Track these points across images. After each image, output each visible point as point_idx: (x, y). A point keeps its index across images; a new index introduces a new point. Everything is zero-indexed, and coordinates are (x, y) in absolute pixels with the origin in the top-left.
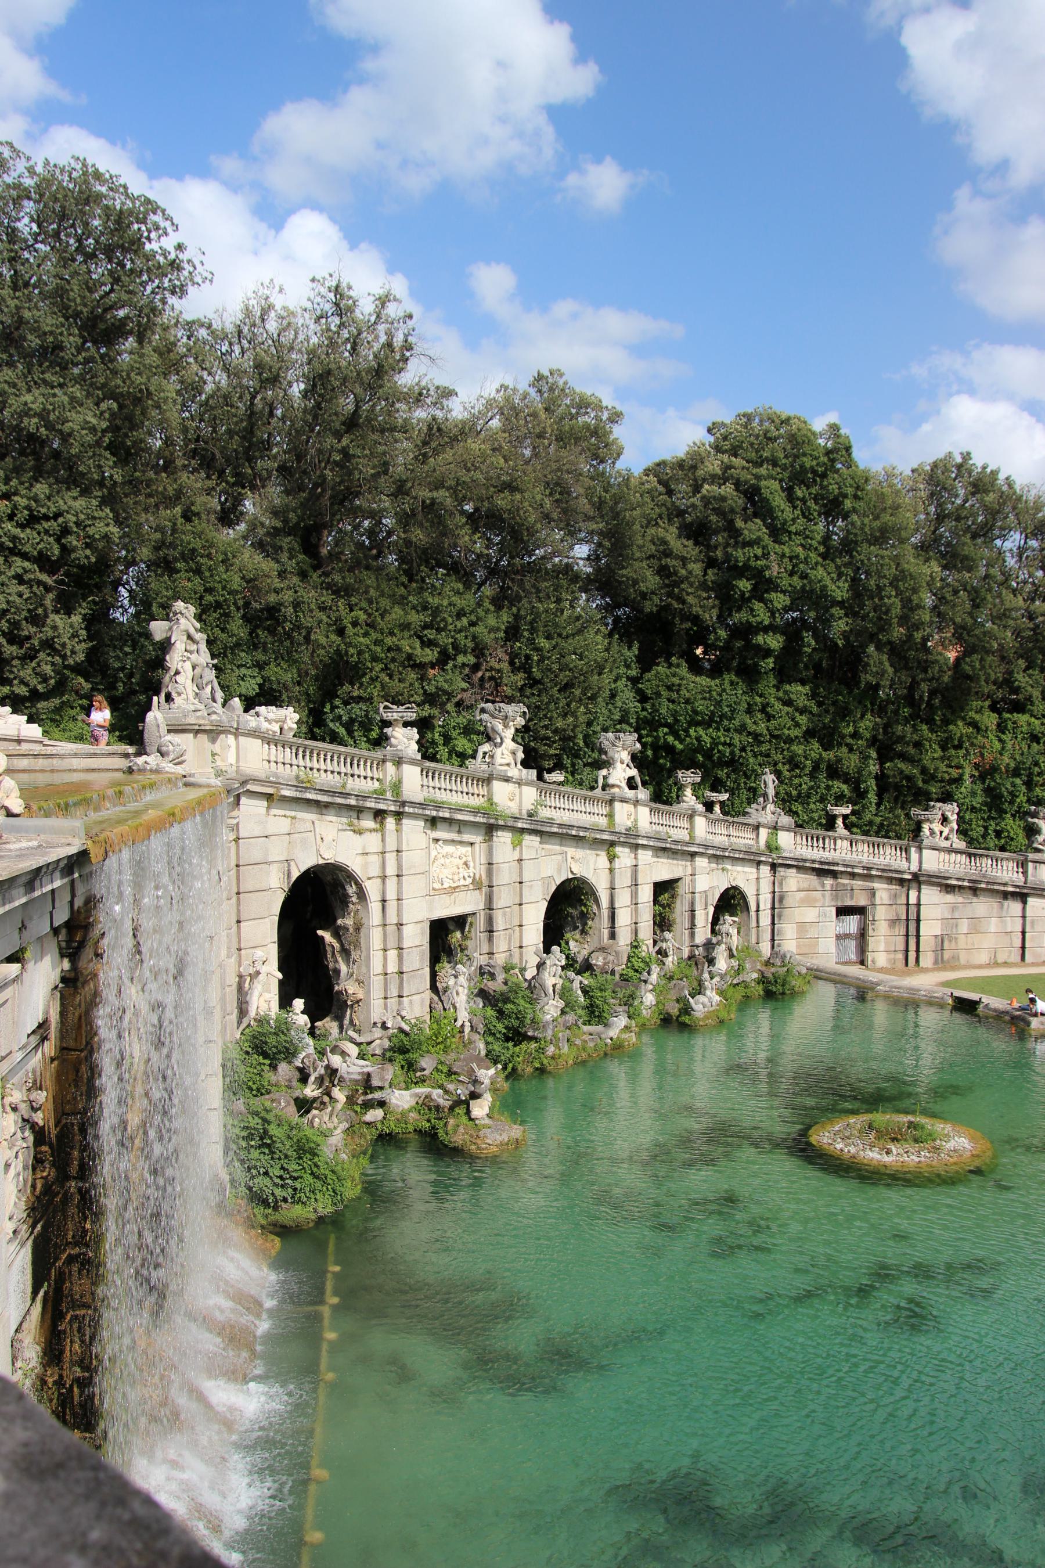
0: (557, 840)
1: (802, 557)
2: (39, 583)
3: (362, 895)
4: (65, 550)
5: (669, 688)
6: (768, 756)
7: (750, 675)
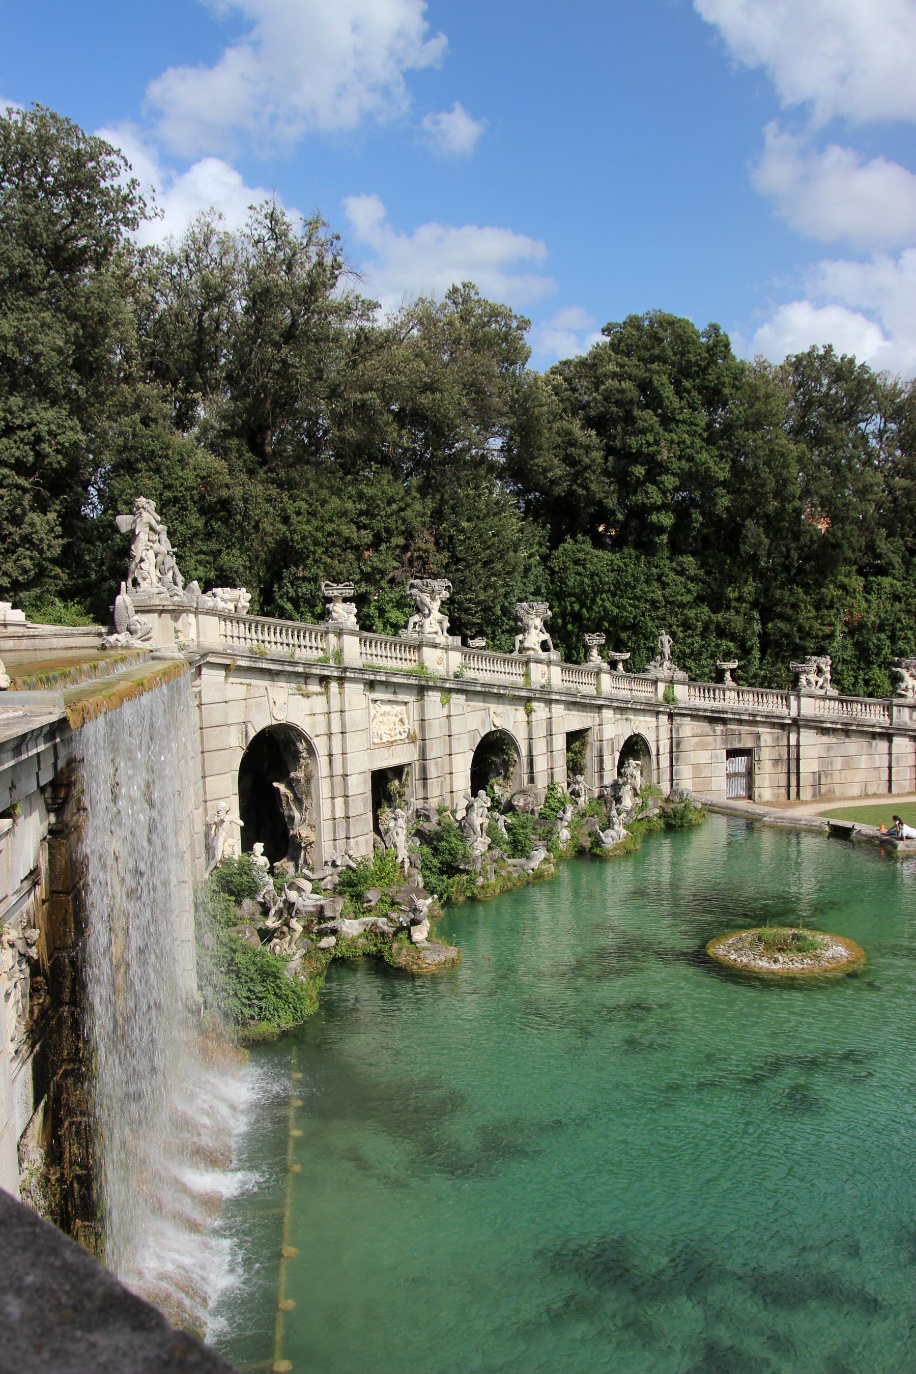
0: (481, 698)
1: (688, 442)
2: (18, 487)
3: (311, 751)
4: (39, 455)
5: (577, 562)
6: (664, 619)
7: (647, 548)
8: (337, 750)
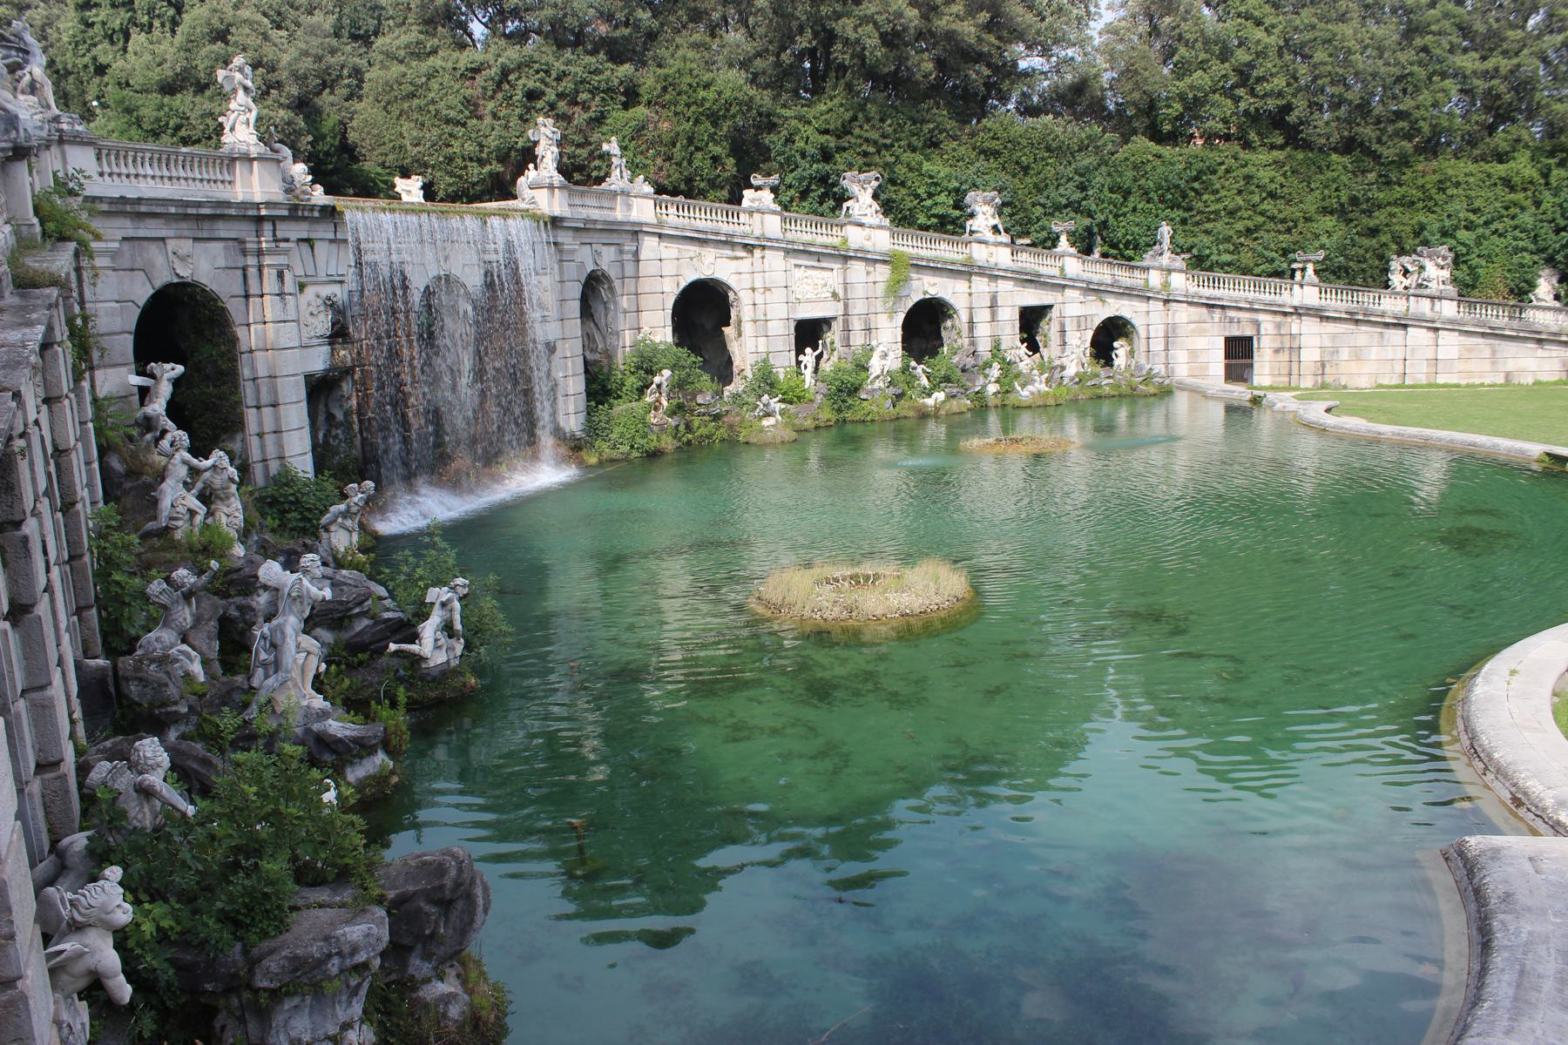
8: (759, 299)
